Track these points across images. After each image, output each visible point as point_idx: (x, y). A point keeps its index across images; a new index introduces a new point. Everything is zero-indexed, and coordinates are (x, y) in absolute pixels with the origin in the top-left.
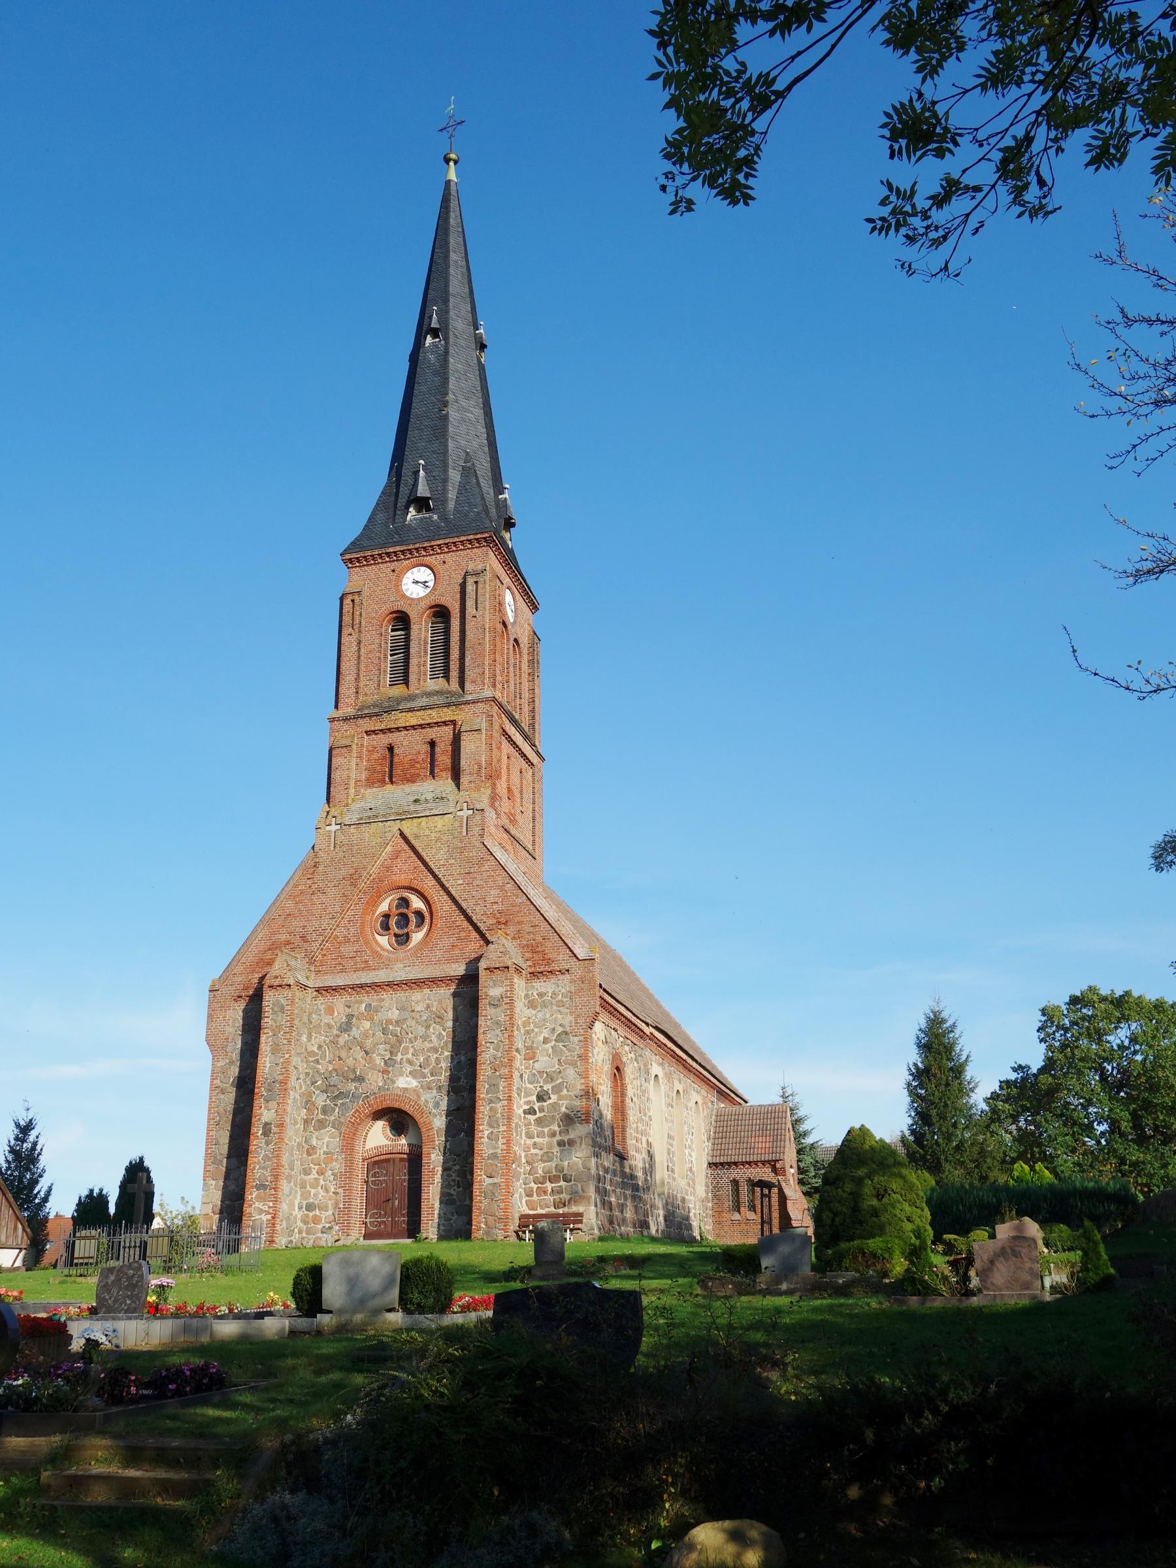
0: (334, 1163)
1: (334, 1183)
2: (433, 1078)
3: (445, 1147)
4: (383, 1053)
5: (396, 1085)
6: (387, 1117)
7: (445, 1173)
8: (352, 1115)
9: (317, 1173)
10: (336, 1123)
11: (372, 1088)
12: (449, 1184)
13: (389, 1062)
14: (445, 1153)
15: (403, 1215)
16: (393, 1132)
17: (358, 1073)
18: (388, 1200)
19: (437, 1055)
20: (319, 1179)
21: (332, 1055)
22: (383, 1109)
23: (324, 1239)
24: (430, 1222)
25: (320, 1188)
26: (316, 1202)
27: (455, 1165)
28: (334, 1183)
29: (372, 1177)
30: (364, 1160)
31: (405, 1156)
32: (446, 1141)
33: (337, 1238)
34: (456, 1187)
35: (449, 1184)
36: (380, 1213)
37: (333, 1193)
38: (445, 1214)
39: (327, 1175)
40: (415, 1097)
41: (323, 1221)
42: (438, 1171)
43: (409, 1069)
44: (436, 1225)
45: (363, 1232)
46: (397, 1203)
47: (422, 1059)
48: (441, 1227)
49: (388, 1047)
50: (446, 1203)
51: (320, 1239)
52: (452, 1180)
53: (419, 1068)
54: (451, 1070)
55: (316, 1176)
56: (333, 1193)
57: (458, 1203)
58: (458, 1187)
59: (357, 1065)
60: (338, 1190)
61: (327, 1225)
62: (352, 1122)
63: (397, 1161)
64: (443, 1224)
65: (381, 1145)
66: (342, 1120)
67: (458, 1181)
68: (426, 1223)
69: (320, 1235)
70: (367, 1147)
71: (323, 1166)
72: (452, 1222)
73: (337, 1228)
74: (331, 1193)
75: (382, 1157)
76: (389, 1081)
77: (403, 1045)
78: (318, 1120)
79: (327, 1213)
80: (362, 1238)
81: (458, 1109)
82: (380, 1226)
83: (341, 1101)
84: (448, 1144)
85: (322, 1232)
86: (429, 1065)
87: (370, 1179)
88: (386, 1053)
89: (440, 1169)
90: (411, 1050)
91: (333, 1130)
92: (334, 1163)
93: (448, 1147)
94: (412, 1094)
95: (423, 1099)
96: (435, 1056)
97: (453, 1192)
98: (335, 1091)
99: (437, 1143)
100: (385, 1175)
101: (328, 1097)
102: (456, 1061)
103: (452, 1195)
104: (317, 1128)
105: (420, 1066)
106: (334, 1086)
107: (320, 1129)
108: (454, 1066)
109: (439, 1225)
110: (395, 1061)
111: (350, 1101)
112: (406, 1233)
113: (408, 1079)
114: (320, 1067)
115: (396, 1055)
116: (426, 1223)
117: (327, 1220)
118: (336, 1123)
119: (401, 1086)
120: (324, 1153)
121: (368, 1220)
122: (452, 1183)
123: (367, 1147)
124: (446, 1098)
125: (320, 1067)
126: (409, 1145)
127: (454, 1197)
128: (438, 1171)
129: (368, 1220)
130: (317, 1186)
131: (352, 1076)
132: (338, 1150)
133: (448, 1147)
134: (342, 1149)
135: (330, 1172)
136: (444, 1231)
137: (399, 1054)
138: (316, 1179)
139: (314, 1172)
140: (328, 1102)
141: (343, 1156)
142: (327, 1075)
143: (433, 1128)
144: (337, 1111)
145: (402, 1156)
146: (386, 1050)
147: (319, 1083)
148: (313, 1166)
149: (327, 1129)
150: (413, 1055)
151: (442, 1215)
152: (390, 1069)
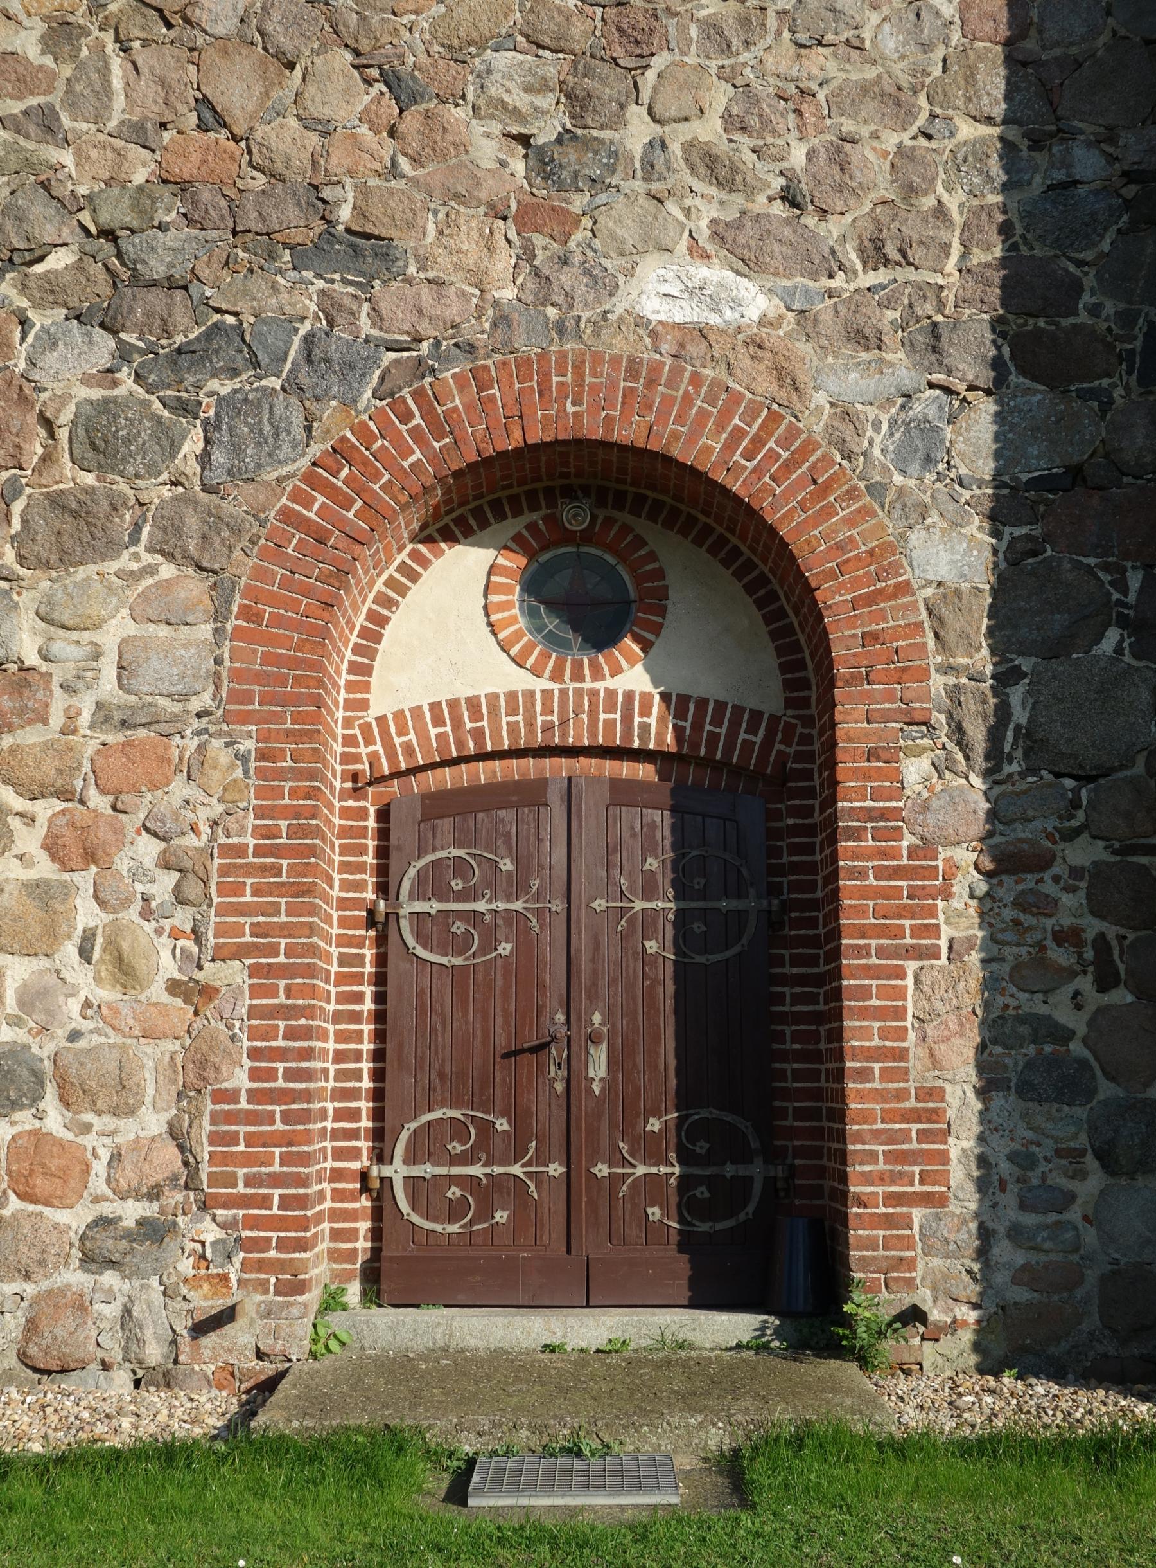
0: (179, 789)
1: (183, 918)
2: (881, 276)
3: (1003, 712)
4: (518, 99)
5: (619, 306)
6: (514, 525)
7: (1010, 887)
8: (310, 478)
9: (52, 846)
10: (192, 523)
11: (453, 312)
12: (1040, 961)
13: (570, 156)
14: (995, 755)
15: (650, 1150)
16: (552, 623)
17: (345, 214)
18: (542, 1047)
19: (906, 138)
20: (67, 891)
21: (147, 88)
22: (530, 451)
23: (111, 1311)
24: (918, 1215)
25: (70, 950)
26: (43, 1050)
27: (1070, 836)
28: (183, 918)
29: (418, 894)
30: (357, 784)
31: (644, 772)
32: (1004, 678)
33: (206, 1303)
34: (1086, 983)
35: (1040, 961)
36: (486, 1128)
37: (174, 987)
38: (1023, 1160)
39: (122, 864)
40: (766, 385)
41: (98, 1183)
42: (953, 868)
43: (711, 212)
44: (968, 1237)
45: (363, 1244)
46: (598, 1065)
47: (798, 156)
48: (1002, 1251)
49: (552, 67)
50: (1026, 1090)
51: (81, 1306)
52: (1060, 937)
53: (778, 209)
54: (1005, 229)
55: (45, 868)
56: (174, 987)
57: (1106, 1089)
58: (1105, 983)
59: (337, 161)
60: (211, 973)
61: (131, 1212)
62: (302, 524)
63: (590, 803)
64: (1015, 1233)
65: (482, 691)
66: (235, 506)
67: (1101, 941)
68: (889, 1221)
69: (74, 1277)
70: (381, 704)
71: (99, 801)
72: (1074, 1214)
73: (211, 1233)
74: (157, 992)
75: (484, 772)
76: (566, 278)
77: (659, 62)
78: (57, 501)
79: (128, 1130)
80: (353, 1292)
81: (1075, 475)
82: (485, 1213)
83: (224, 387)
84: (1017, 694)
85: (93, 1260)
86: (848, 189)
87: (409, 907)
88: (546, 101)
89: (965, 856)
90: (720, 96)
91: (167, 571)
92: (179, 789)
93: (1020, 716)
94: (743, 359)
95: (820, 398)
96: (891, 140)
97: (1065, 1016)
98: (181, 317)
99: (938, 683)
100: (518, 887)
101: (124, 354)
102: (1038, 183)
103: (1063, 1035)
104: (43, 546)
105: (790, 198)
106: (171, 284)
107: (66, 560)
108: (1028, 216)
109: (985, 1234)
110: (615, 157)
111: (292, 387)
112: (682, 1265)
113: (702, 272)
114: (67, 157)
115: (618, 121)
116: (889, 1221)
117: (128, 1176)
118: (192, 523)
119: (653, 308)
120: (103, 715)
121: (397, 1170)
122: (1060, 956)
123: (381, 704)
124: (985, 407)
125: (67, 157)
126: (676, 703)
127: (1076, 1047)
128: (953, 868)
129: (397, 1170)
130: (52, 937)
131: (305, 231)
132: (205, 700)
133: (1020, 716)
134: (236, 697)
135: (148, 849)
136: (1025, 1275)
137: (636, 114)
138: (38, 889)
139: (29, 841)
140: (127, 384)
141: (249, 745)
142: (115, 213)
143: (904, 588)
144: (193, 444)
145: (626, 769)
146: (543, 87)
147: (58, 260)
148: (18, 803)
149: (125, 561)
150: (733, 123)
151: (1005, 1167)
152: (578, 203)
